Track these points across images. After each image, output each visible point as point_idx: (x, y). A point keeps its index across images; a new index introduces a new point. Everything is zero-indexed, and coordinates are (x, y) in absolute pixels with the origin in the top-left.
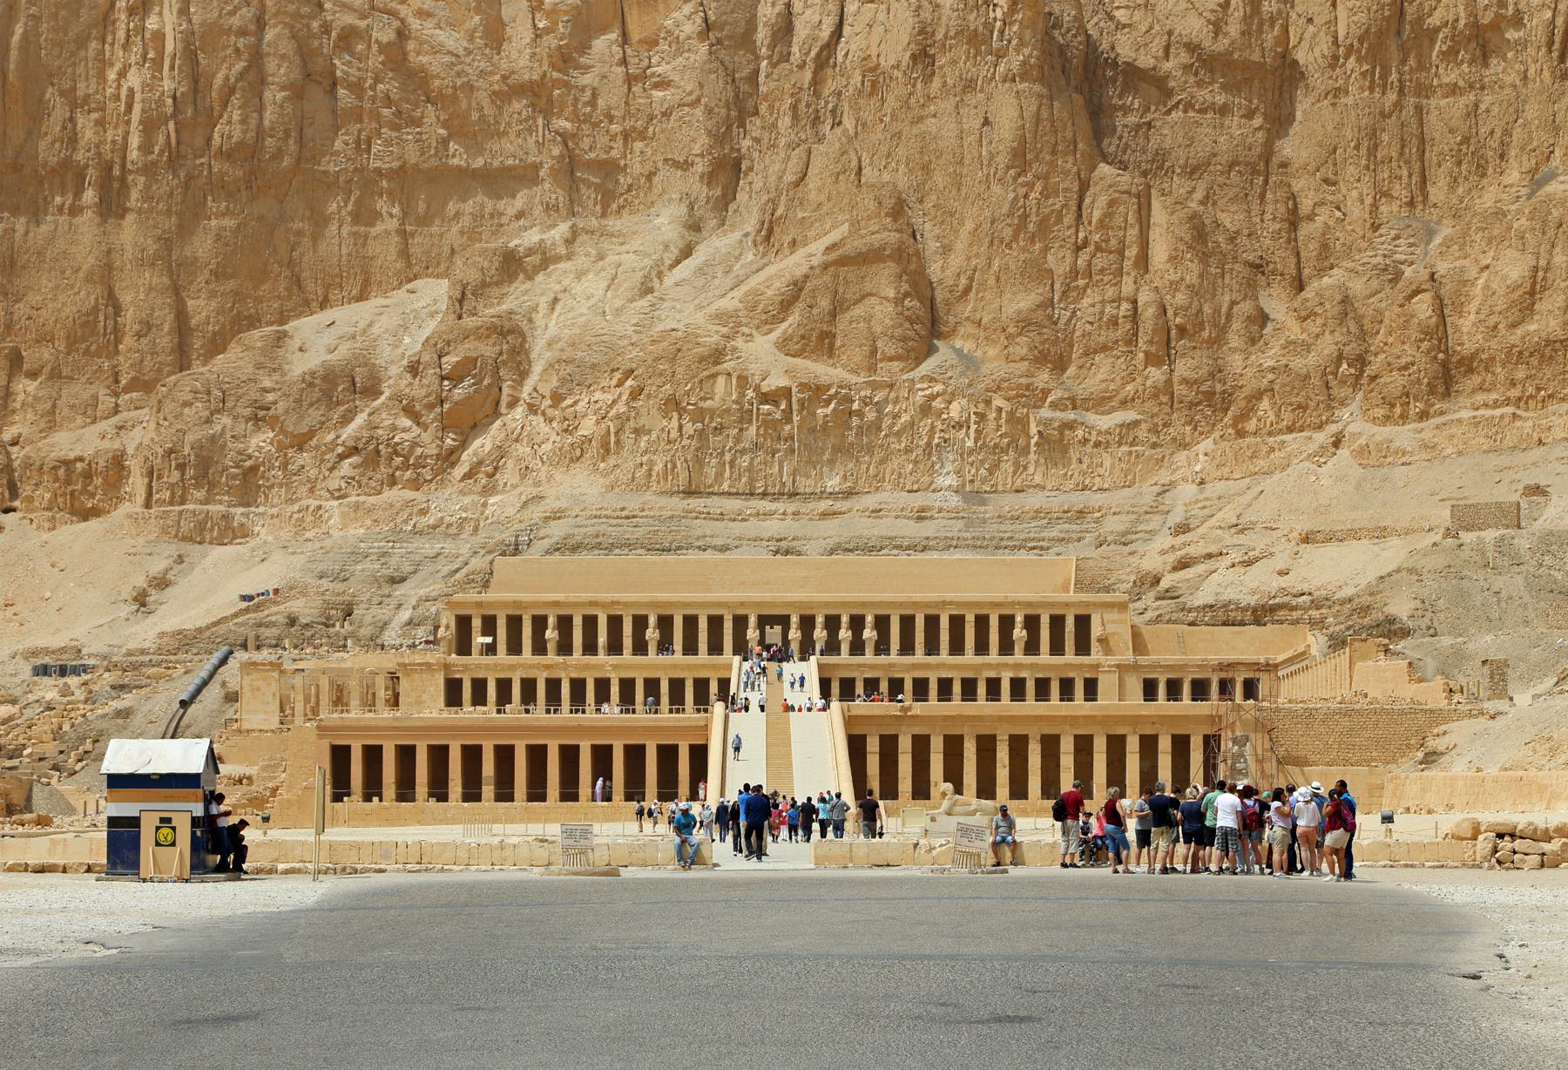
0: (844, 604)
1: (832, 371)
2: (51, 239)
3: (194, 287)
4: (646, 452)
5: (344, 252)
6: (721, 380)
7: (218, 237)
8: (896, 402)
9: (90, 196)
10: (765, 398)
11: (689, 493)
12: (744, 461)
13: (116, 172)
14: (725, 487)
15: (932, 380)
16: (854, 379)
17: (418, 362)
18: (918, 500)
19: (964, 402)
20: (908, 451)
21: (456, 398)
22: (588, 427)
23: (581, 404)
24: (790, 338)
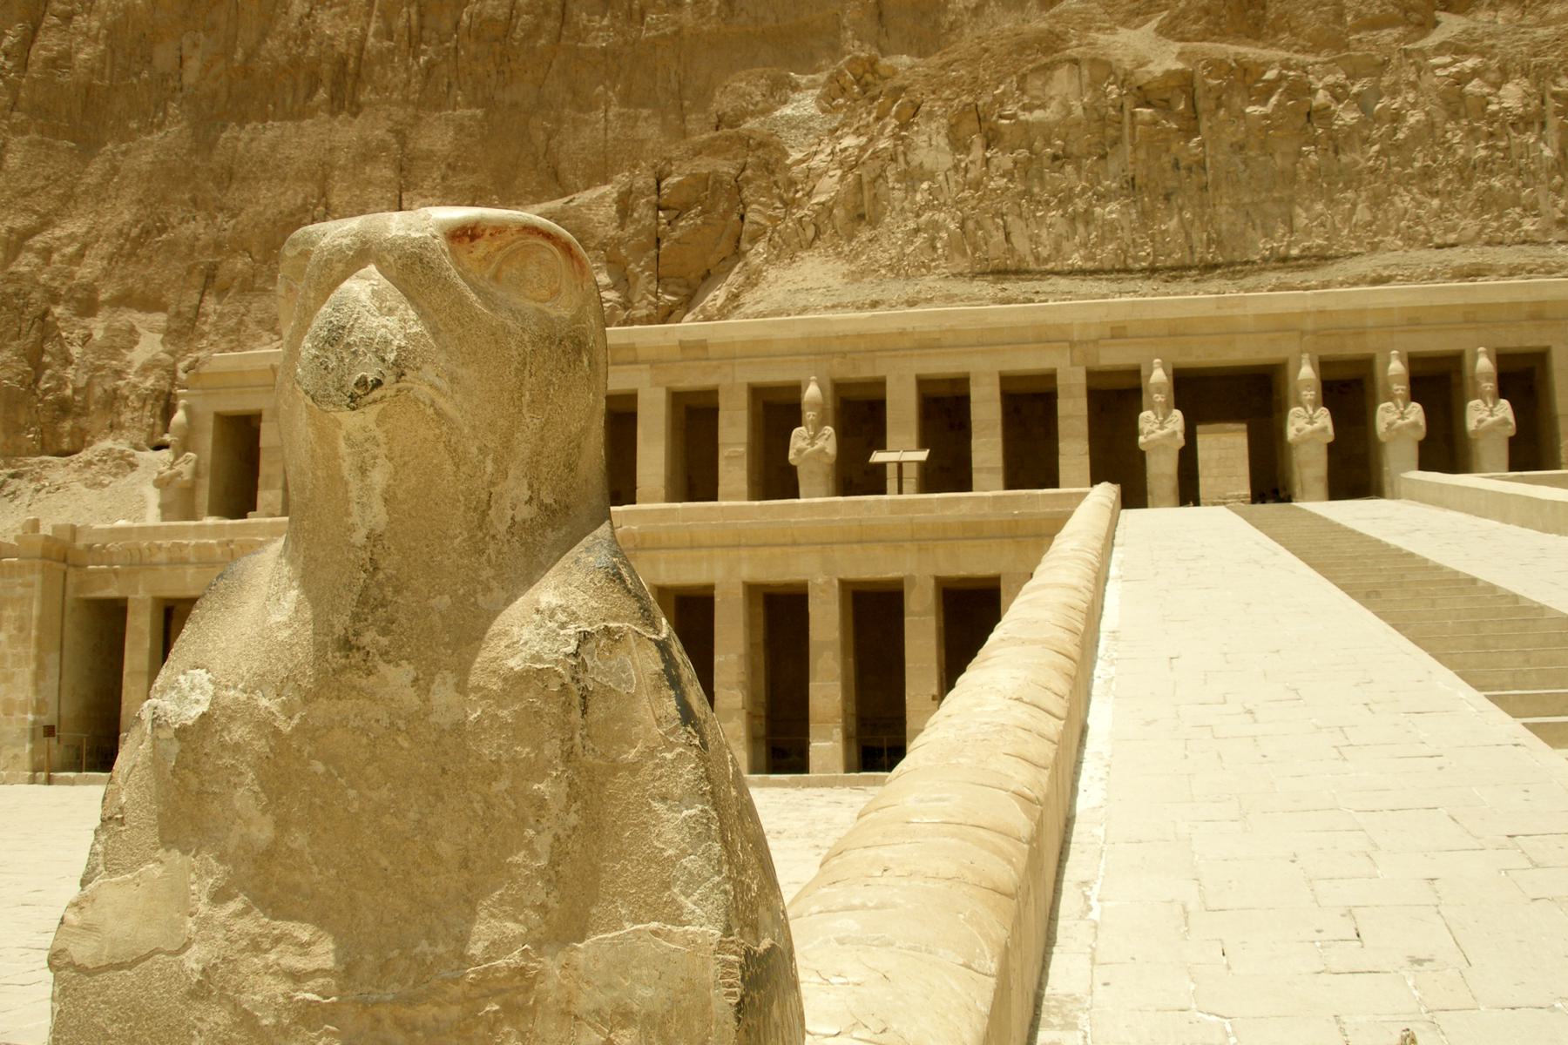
0: (1472, 316)
1: (1264, 52)
2: (273, 148)
3: (427, 184)
4: (928, 206)
5: (610, 135)
6: (1062, 74)
7: (460, 128)
8: (1394, 92)
9: (322, 94)
10: (1144, 96)
11: (1001, 273)
12: (1113, 206)
13: (351, 64)
14: (1076, 260)
15: (1458, 49)
16: (1311, 59)
17: (630, 192)
18: (1458, 257)
19: (1525, 83)
20: (1427, 174)
21: (676, 234)
22: (828, 188)
23: (822, 156)
24: (1183, 14)
